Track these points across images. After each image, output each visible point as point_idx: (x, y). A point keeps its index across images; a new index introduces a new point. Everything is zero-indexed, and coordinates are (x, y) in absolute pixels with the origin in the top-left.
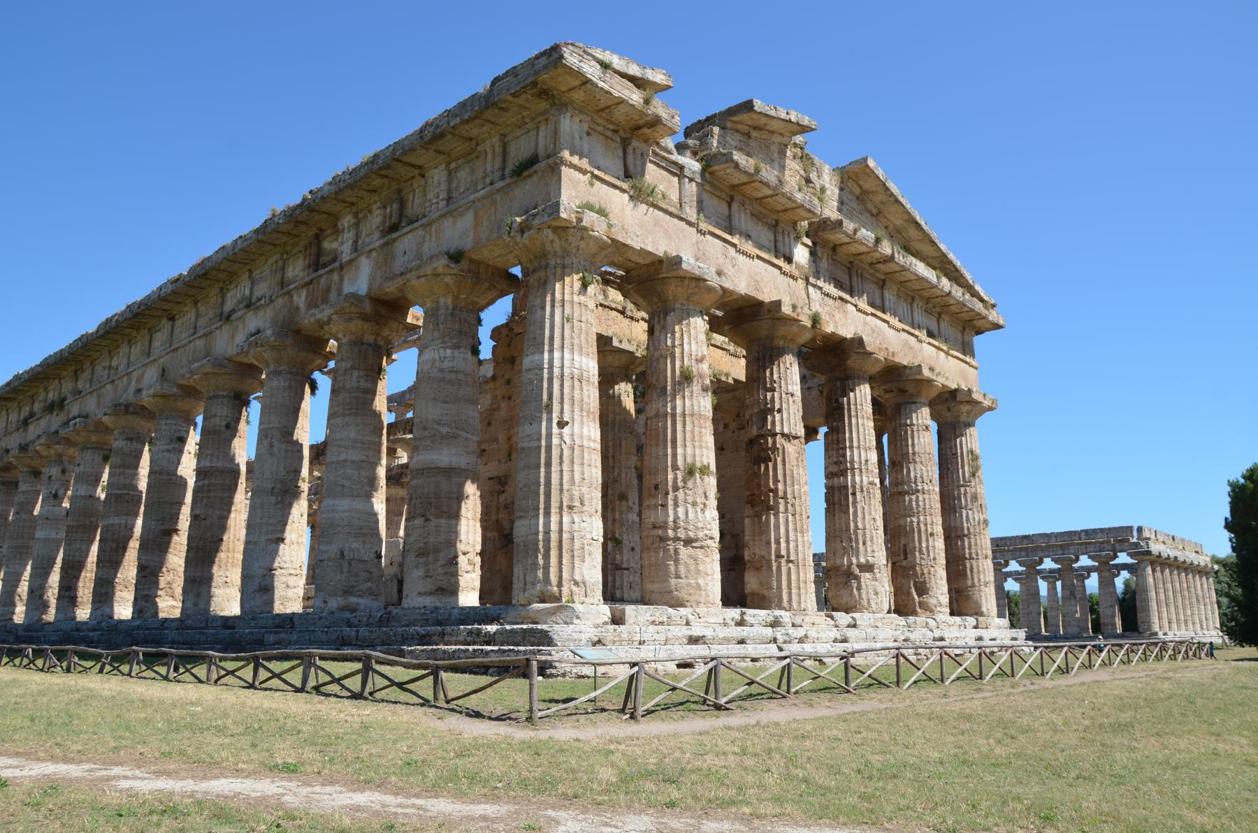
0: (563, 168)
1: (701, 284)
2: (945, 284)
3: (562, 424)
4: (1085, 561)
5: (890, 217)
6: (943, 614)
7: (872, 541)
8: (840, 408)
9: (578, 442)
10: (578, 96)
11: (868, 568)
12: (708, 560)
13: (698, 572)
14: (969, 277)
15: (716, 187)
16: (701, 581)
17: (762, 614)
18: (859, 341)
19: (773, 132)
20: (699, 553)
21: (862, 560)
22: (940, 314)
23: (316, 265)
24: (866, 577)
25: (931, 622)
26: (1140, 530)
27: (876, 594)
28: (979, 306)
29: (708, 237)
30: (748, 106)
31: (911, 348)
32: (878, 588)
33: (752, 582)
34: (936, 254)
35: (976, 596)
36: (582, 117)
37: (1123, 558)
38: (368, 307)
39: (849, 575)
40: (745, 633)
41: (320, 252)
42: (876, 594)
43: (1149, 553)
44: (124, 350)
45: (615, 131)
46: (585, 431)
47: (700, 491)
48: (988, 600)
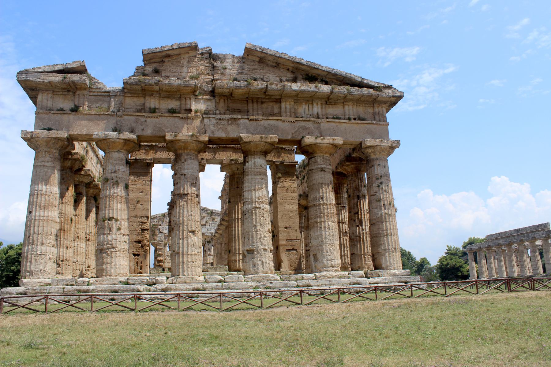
1: (108, 141)
2: (325, 88)
5: (285, 64)
9: (37, 218)
10: (39, 86)
12: (109, 257)
15: (134, 94)
19: (180, 54)
20: (105, 255)
22: (343, 103)
29: (125, 117)
31: (306, 129)
34: (326, 73)
36: (47, 92)
40: (117, 288)
45: (69, 91)
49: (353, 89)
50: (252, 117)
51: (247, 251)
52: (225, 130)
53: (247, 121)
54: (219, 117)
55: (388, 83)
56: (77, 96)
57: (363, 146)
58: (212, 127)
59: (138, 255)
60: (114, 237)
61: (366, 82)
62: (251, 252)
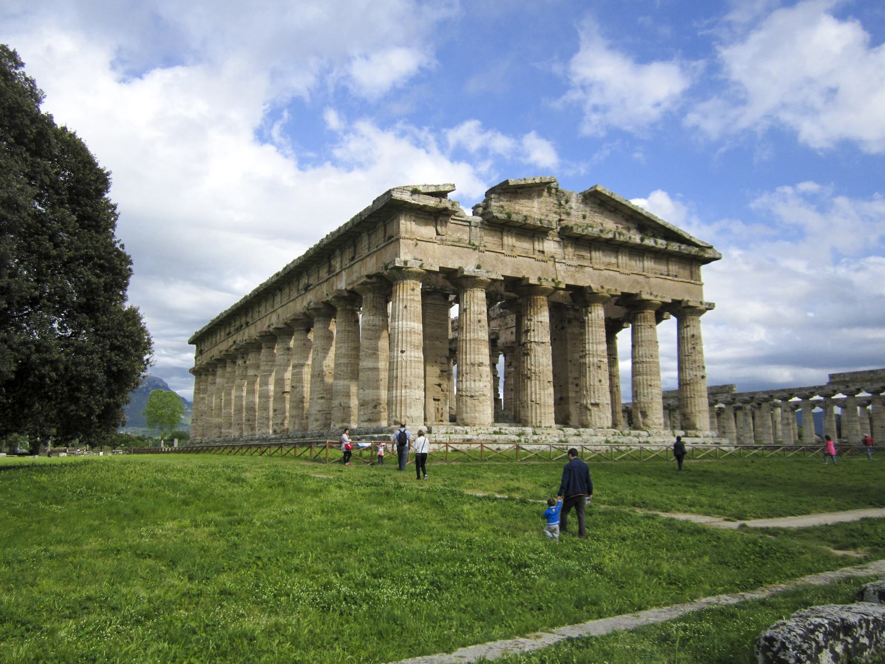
0: (401, 240)
2: (661, 243)
3: (402, 352)
7: (598, 390)
8: (584, 322)
13: (475, 411)
16: (477, 415)
17: (515, 429)
18: (590, 287)
20: (476, 402)
21: (593, 402)
23: (329, 272)
24: (594, 409)
25: (645, 433)
27: (600, 418)
28: (694, 250)
31: (638, 283)
35: (693, 419)
38: (346, 294)
39: (586, 408)
41: (330, 266)
42: (600, 418)
44: (264, 304)
46: (413, 354)
47: (477, 374)
49: (683, 247)
50: (596, 266)
51: (592, 404)
52: (572, 276)
53: (591, 269)
54: (569, 263)
55: (710, 244)
56: (439, 222)
57: (683, 305)
58: (562, 273)
59: (438, 400)
60: (485, 384)
61: (693, 240)
62: (596, 405)
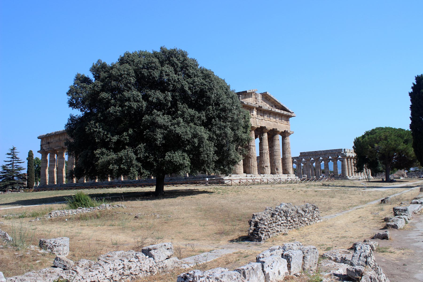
2: (282, 112)
4: (330, 157)
6: (281, 174)
8: (262, 138)
11: (267, 166)
14: (288, 108)
17: (249, 175)
24: (266, 168)
26: (344, 150)
28: (289, 114)
30: (246, 91)
32: (268, 170)
33: (247, 170)
37: (340, 157)
39: (264, 168)
43: (346, 156)
48: (291, 171)
49: (287, 112)
52: (260, 123)
